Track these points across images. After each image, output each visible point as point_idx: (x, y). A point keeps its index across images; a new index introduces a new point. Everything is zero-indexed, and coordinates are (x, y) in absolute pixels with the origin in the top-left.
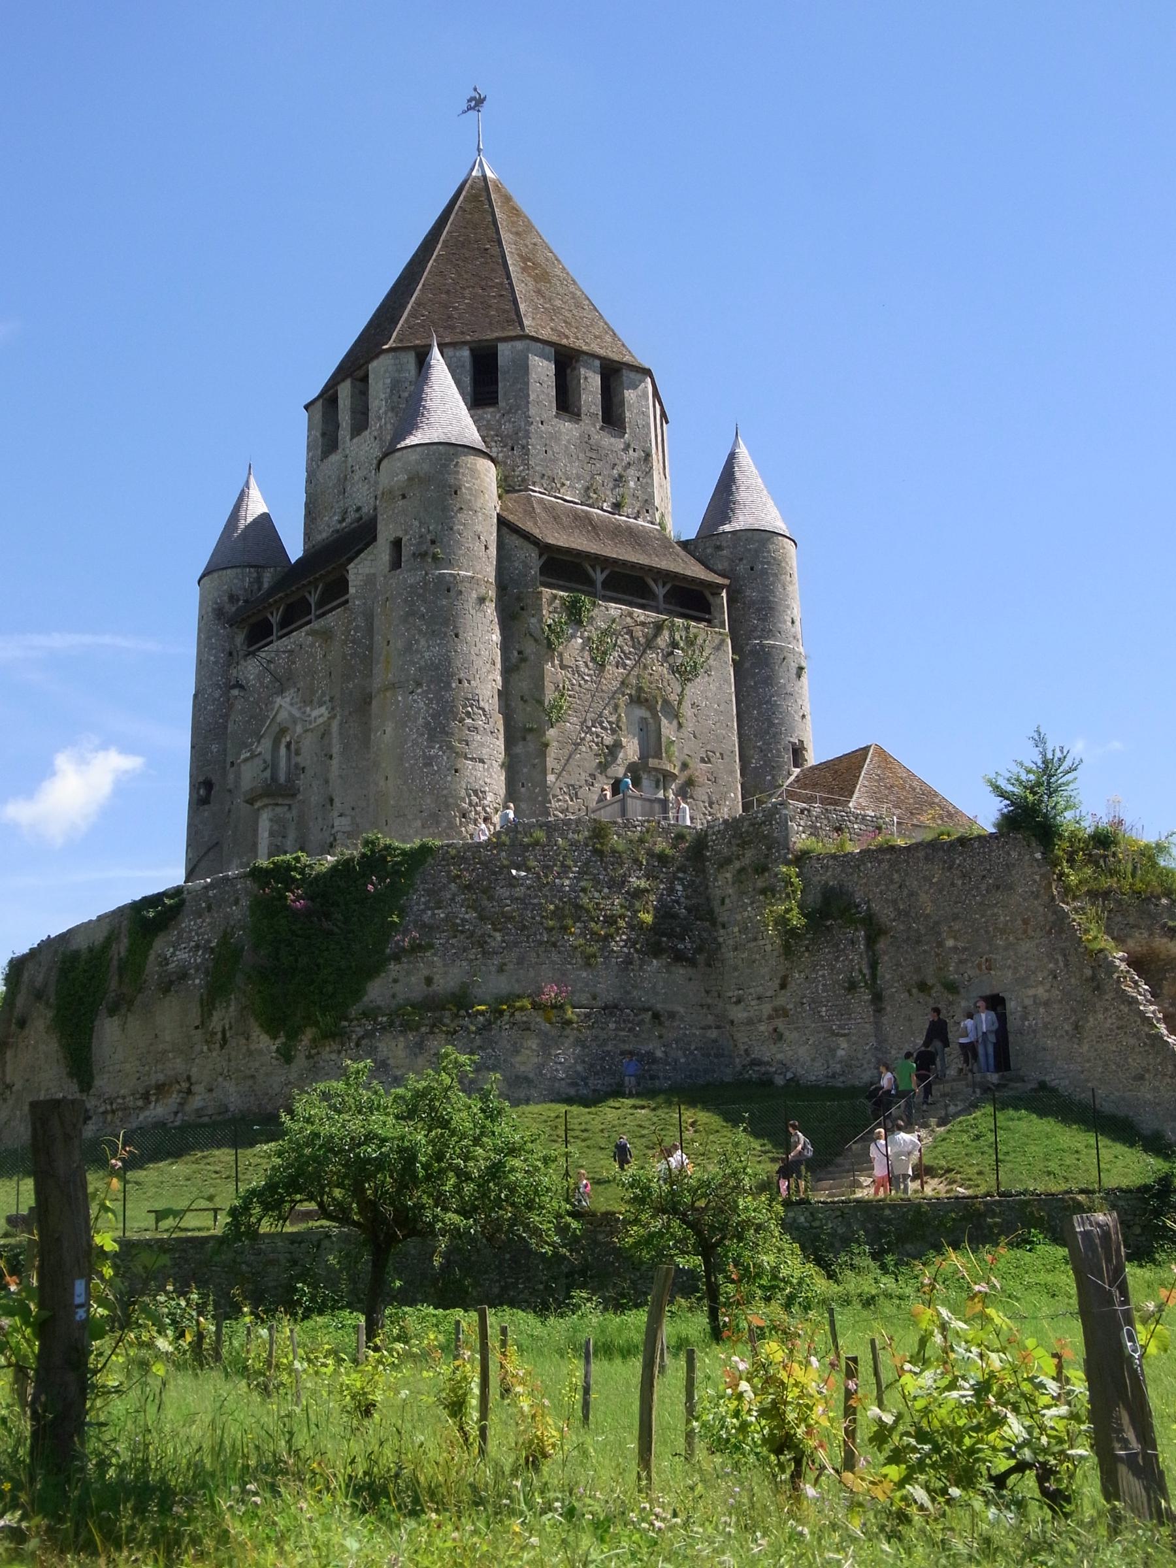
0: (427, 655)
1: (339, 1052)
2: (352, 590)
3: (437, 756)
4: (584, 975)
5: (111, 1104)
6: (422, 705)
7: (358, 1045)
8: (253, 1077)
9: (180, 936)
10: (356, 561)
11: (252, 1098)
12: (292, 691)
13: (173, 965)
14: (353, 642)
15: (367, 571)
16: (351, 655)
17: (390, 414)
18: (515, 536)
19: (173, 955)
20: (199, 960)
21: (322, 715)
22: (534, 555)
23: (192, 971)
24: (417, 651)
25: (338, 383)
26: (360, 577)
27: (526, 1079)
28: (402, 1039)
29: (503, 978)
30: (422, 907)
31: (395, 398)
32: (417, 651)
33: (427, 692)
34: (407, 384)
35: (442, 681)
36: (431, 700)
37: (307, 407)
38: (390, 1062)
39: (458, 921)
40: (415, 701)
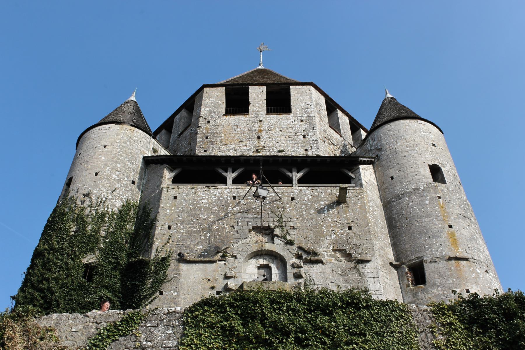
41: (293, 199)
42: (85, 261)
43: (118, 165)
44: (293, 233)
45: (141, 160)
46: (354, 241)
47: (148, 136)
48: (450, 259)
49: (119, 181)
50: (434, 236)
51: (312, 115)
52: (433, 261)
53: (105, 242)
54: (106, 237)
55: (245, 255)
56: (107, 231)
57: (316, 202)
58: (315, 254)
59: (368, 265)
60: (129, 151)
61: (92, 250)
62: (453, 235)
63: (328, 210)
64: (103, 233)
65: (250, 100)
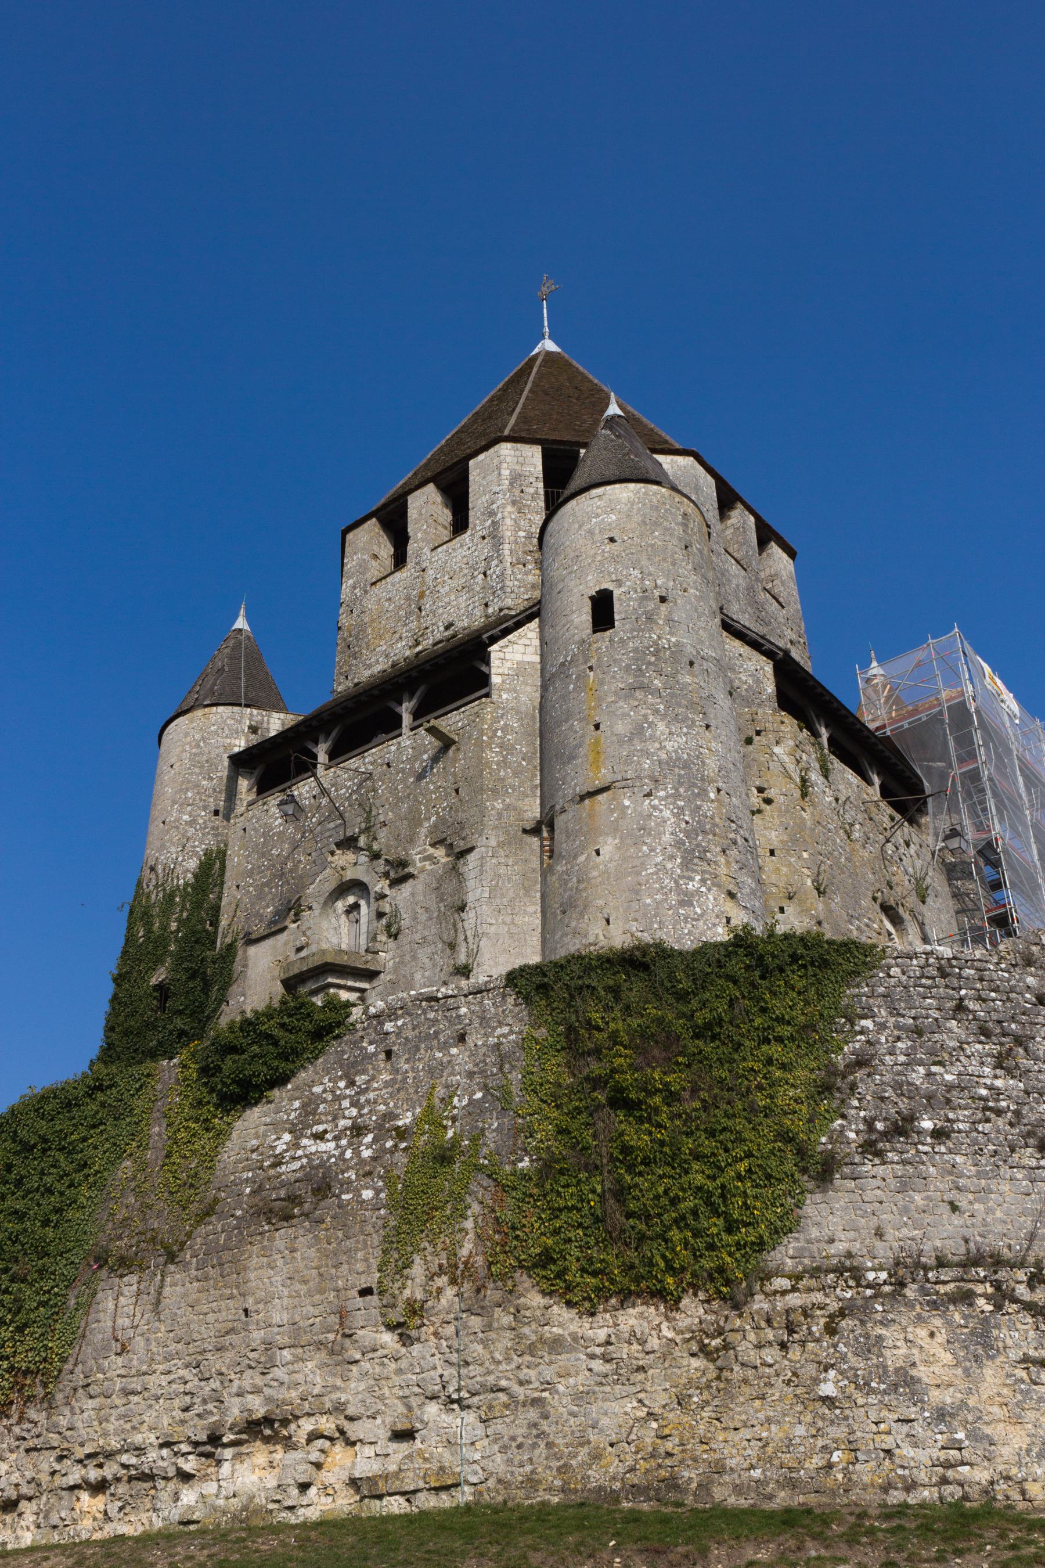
0: (669, 746)
2: (495, 680)
3: (698, 891)
6: (667, 814)
7: (831, 1330)
8: (536, 1402)
9: (309, 1109)
10: (502, 643)
11: (542, 1450)
13: (296, 1165)
14: (501, 746)
15: (518, 657)
16: (498, 764)
17: (509, 508)
18: (737, 643)
20: (366, 1153)
22: (769, 668)
23: (352, 1175)
24: (653, 738)
25: (411, 491)
26: (509, 664)
28: (938, 1322)
30: (902, 1059)
31: (517, 492)
32: (653, 738)
33: (676, 796)
34: (532, 480)
35: (695, 785)
36: (681, 809)
38: (921, 1372)
39: (984, 1092)
40: (655, 808)
41: (388, 765)
42: (153, 981)
43: (190, 794)
44: (383, 834)
45: (226, 763)
46: (461, 816)
47: (236, 709)
48: (582, 798)
49: (192, 823)
50: (572, 758)
51: (499, 515)
52: (563, 811)
53: (177, 940)
54: (178, 931)
55: (322, 900)
56: (179, 920)
57: (416, 761)
58: (403, 864)
59: (472, 857)
60: (205, 758)
61: (160, 961)
62: (597, 742)
63: (432, 768)
64: (174, 926)
65: (410, 530)
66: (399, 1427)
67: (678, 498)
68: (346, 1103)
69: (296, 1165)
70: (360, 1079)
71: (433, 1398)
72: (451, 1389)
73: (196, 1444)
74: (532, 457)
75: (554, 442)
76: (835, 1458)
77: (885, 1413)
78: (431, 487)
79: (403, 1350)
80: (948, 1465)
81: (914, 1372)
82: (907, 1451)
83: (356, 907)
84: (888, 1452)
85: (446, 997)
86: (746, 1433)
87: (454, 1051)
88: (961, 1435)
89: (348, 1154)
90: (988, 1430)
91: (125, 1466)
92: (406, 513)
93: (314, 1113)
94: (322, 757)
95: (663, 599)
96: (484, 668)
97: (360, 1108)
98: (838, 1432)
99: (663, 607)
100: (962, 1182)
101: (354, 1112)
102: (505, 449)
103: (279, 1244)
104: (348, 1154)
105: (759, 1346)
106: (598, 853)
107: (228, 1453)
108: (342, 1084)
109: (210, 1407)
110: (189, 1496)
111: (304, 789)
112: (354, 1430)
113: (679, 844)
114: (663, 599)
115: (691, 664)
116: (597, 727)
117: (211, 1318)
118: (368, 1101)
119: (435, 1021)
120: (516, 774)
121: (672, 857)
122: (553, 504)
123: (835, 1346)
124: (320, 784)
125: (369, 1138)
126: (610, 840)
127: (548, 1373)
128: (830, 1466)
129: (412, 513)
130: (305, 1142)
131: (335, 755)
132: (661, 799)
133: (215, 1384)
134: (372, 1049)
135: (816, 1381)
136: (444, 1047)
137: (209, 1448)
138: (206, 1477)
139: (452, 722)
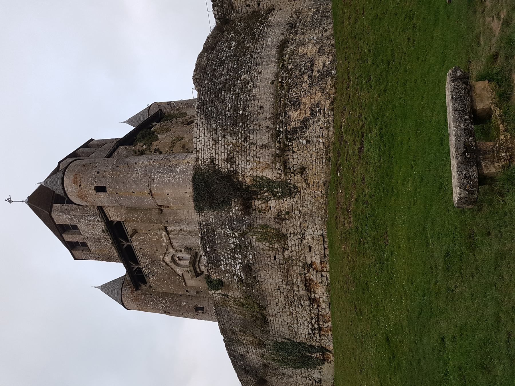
0: (140, 174)
1: (294, 152)
2: (119, 219)
3: (180, 169)
4: (270, 39)
5: (315, 329)
6: (159, 175)
12: (158, 254)
13: (242, 275)
15: (113, 213)
19: (237, 276)
21: (165, 235)
27: (320, 49)
29: (264, 71)
30: (224, 117)
31: (66, 211)
37: (75, 259)
39: (233, 97)
40: (157, 179)
66: (308, 250)
67: (70, 167)
68: (227, 262)
69: (242, 275)
70: (222, 258)
71: (302, 241)
72: (300, 237)
73: (310, 303)
74: (56, 206)
75: (52, 200)
76: (321, 141)
77: (311, 128)
78: (64, 235)
79: (290, 249)
80: (324, 113)
81: (302, 120)
82: (320, 123)
83: (178, 257)
84: (320, 128)
85: (201, 234)
86: (314, 163)
87: (216, 233)
88: (317, 109)
89: (240, 261)
90: (317, 102)
91: (315, 323)
92: (71, 242)
93: (229, 270)
94: (137, 266)
95: (98, 173)
96: (115, 222)
97: (228, 258)
98: (315, 140)
99: (101, 173)
100: (256, 105)
101: (230, 259)
102: (53, 215)
103: (262, 280)
104: (240, 261)
105: (293, 159)
106: (168, 194)
107: (313, 295)
108: (222, 262)
109: (301, 299)
110: (323, 305)
111: (146, 271)
112: (309, 262)
113: (167, 173)
114: (98, 173)
115: (117, 166)
116: (133, 192)
117: (279, 298)
118: (227, 256)
119: (208, 237)
120: (145, 215)
121: (170, 175)
122: (70, 202)
123: (294, 140)
124: (145, 267)
125: (236, 256)
126: (165, 191)
127: (297, 212)
128: (323, 143)
129: (71, 240)
130: (237, 273)
131: (137, 263)
132: (154, 177)
133: (296, 298)
134: (214, 254)
135: (303, 144)
136: (215, 235)
137: (312, 300)
138: (319, 301)
139: (129, 231)
